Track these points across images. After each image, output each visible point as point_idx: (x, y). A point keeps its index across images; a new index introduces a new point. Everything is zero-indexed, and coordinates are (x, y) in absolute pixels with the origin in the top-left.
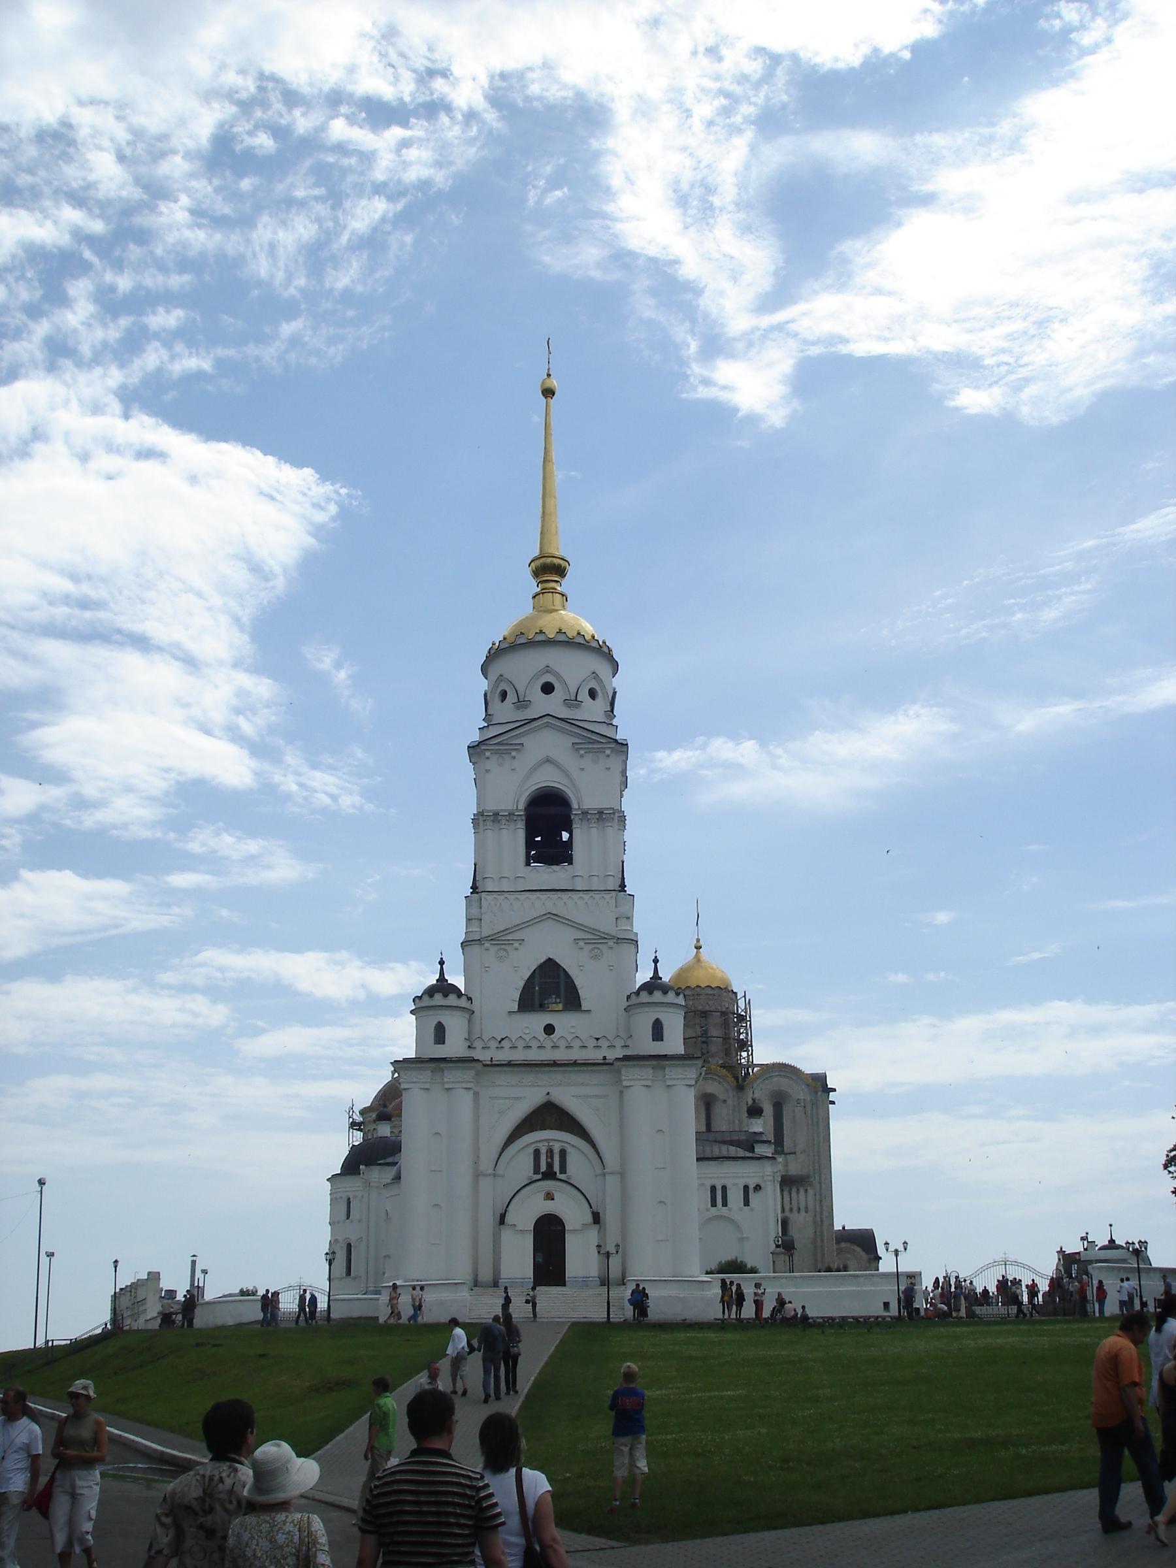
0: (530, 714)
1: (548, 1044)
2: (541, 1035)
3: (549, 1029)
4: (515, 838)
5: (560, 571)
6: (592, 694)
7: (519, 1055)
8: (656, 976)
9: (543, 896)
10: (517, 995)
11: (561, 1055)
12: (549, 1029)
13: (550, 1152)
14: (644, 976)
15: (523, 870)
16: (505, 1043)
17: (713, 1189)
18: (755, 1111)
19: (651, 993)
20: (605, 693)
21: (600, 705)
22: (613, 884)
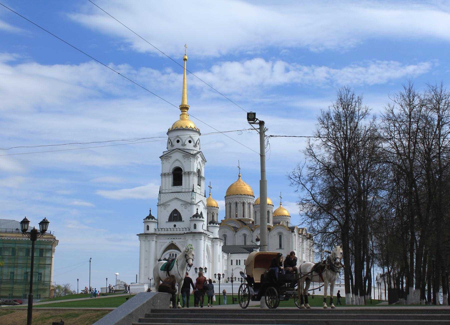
0: (174, 148)
1: (172, 229)
2: (173, 227)
3: (175, 226)
4: (170, 180)
5: (187, 108)
6: (190, 142)
7: (166, 232)
8: (197, 213)
9: (174, 194)
10: (168, 218)
11: (178, 232)
12: (175, 226)
13: (173, 254)
14: (195, 213)
15: (171, 187)
16: (163, 230)
17: (237, 261)
18: (257, 240)
19: (197, 217)
20: (194, 141)
21: (192, 143)
22: (191, 190)
